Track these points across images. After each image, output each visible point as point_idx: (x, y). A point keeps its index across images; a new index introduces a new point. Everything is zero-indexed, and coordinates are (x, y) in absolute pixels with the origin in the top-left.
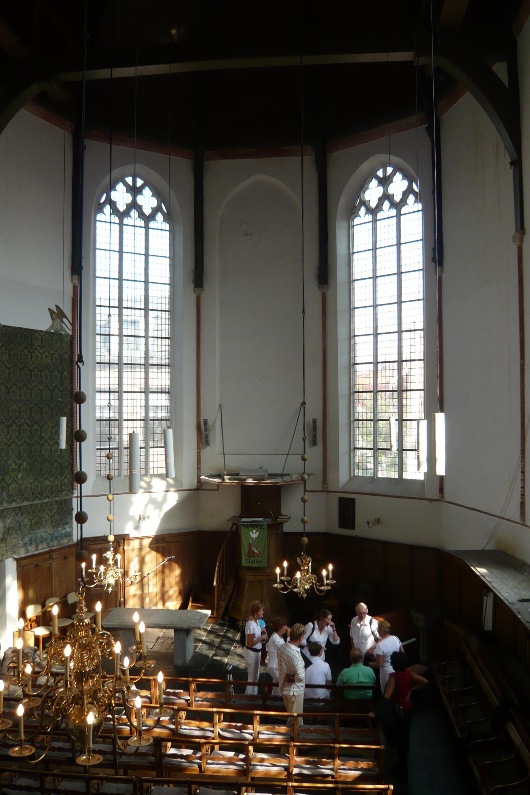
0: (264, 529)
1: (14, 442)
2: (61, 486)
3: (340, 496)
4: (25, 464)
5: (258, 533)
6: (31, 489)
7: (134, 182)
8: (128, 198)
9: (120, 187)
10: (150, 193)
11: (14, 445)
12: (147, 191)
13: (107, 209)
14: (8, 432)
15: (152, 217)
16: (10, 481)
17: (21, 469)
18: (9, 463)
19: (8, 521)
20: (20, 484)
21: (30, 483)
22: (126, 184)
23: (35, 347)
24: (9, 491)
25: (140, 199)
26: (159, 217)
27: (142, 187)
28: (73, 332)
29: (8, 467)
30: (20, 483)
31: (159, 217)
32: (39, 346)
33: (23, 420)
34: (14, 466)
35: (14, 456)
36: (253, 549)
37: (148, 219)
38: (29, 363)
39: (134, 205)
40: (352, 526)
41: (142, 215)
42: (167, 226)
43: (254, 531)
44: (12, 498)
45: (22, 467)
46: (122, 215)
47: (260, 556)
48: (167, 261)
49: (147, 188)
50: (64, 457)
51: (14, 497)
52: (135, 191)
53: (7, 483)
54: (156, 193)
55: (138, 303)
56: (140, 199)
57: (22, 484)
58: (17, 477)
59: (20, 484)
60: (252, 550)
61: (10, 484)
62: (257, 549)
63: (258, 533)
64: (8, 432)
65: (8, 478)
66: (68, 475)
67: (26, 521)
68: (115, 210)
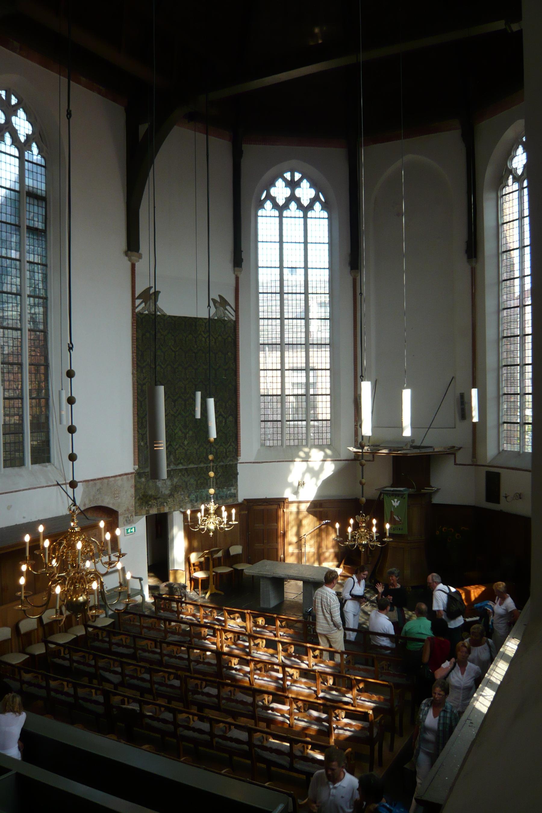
0: (404, 498)
1: (180, 414)
2: (226, 453)
3: (487, 470)
4: (191, 433)
5: (399, 502)
6: (197, 454)
7: (293, 176)
8: (287, 192)
9: (280, 183)
10: (308, 185)
11: (180, 416)
12: (305, 184)
13: (268, 205)
14: (175, 406)
15: (310, 207)
16: (177, 447)
17: (187, 437)
18: (176, 431)
19: (175, 480)
20: (186, 449)
21: (195, 448)
22: (285, 179)
23: (199, 332)
24: (176, 455)
25: (298, 192)
26: (317, 206)
27: (301, 180)
28: (236, 318)
29: (175, 434)
30: (186, 448)
31: (317, 206)
32: (203, 332)
33: (188, 395)
34: (180, 434)
35: (180, 426)
36: (395, 517)
37: (306, 209)
38: (193, 347)
39: (293, 198)
40: (498, 501)
41: (300, 206)
42: (325, 214)
43: (396, 500)
44: (179, 461)
45: (187, 435)
46: (281, 209)
47: (401, 524)
48: (326, 247)
49: (305, 181)
50: (228, 428)
51: (181, 460)
52: (293, 185)
53: (174, 448)
54: (313, 185)
55: (298, 288)
56: (298, 192)
57: (188, 450)
58: (183, 443)
59: (186, 449)
60: (394, 517)
61: (177, 449)
62: (398, 517)
63: (399, 502)
64: (175, 406)
65: (175, 444)
66: (233, 444)
67: (192, 481)
68: (275, 206)
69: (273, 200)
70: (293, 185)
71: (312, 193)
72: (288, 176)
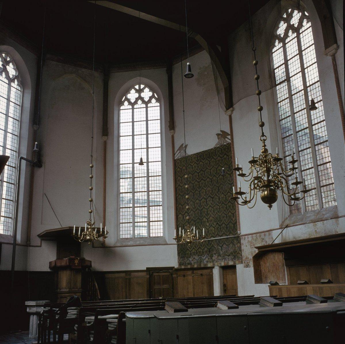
7: (140, 87)
8: (137, 95)
9: (133, 91)
10: (148, 90)
12: (147, 90)
13: (126, 103)
15: (150, 101)
25: (142, 95)
26: (153, 100)
27: (144, 88)
31: (153, 100)
37: (147, 103)
39: (140, 98)
41: (144, 102)
42: (158, 104)
46: (133, 104)
52: (139, 91)
54: (151, 89)
56: (142, 95)
68: (130, 103)
69: (128, 100)
70: (139, 91)
71: (151, 94)
72: (137, 87)
